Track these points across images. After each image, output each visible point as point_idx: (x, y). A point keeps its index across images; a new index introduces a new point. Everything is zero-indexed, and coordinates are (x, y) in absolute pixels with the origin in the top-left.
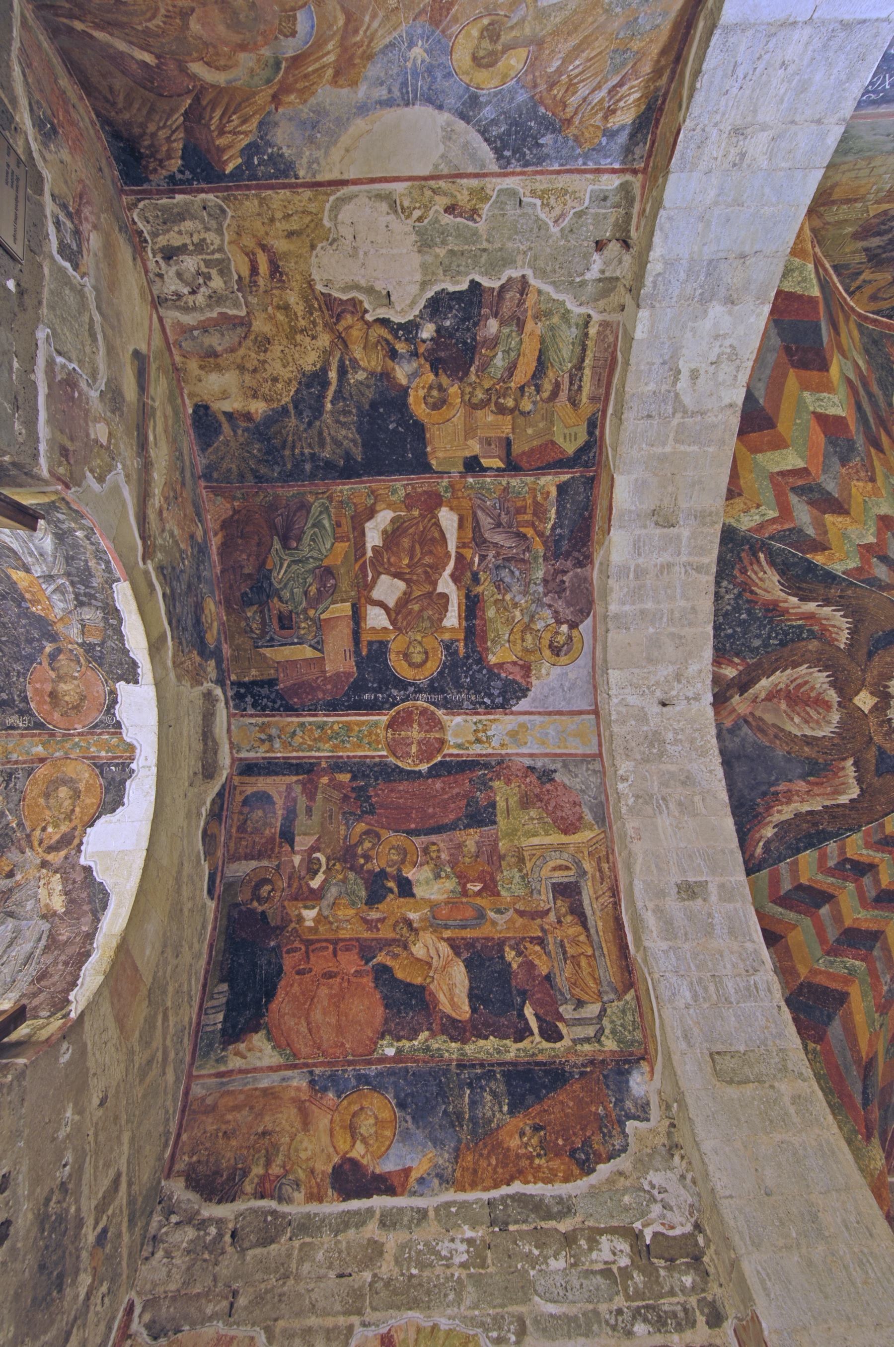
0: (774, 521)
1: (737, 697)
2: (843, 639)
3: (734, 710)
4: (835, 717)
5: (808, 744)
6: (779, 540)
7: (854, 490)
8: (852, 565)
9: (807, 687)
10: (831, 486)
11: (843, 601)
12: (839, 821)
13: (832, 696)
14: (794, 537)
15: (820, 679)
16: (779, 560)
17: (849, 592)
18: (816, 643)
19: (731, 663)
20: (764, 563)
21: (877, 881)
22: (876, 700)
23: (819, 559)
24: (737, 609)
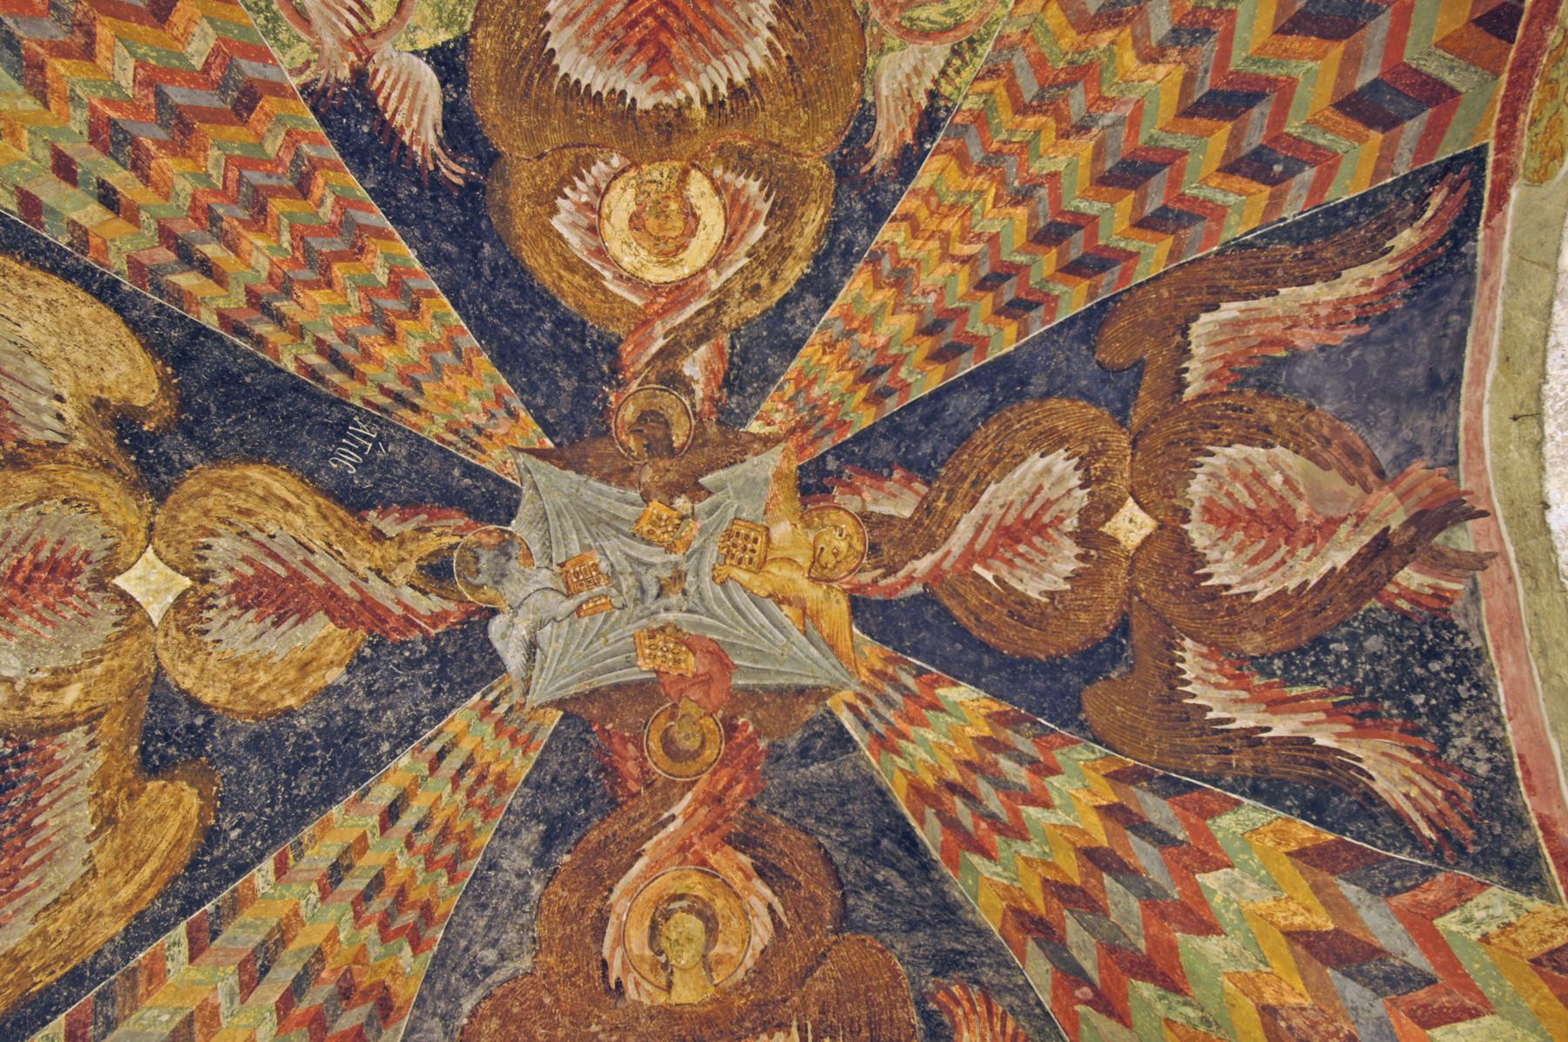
0: (1440, 910)
1: (1394, 526)
2: (1191, 659)
3: (1402, 497)
4: (1198, 488)
5: (1267, 430)
6: (1405, 870)
7: (1300, 986)
8: (1226, 825)
9: (1252, 551)
10: (1353, 991)
11: (1217, 741)
12: (1255, 266)
13: (1199, 534)
14: (1379, 877)
15: (1225, 569)
16: (1387, 823)
17: (1210, 762)
18: (1248, 649)
19: (1414, 598)
20: (1416, 817)
21: (1235, 138)
22: (1107, 529)
23: (1305, 832)
24: (1438, 715)
